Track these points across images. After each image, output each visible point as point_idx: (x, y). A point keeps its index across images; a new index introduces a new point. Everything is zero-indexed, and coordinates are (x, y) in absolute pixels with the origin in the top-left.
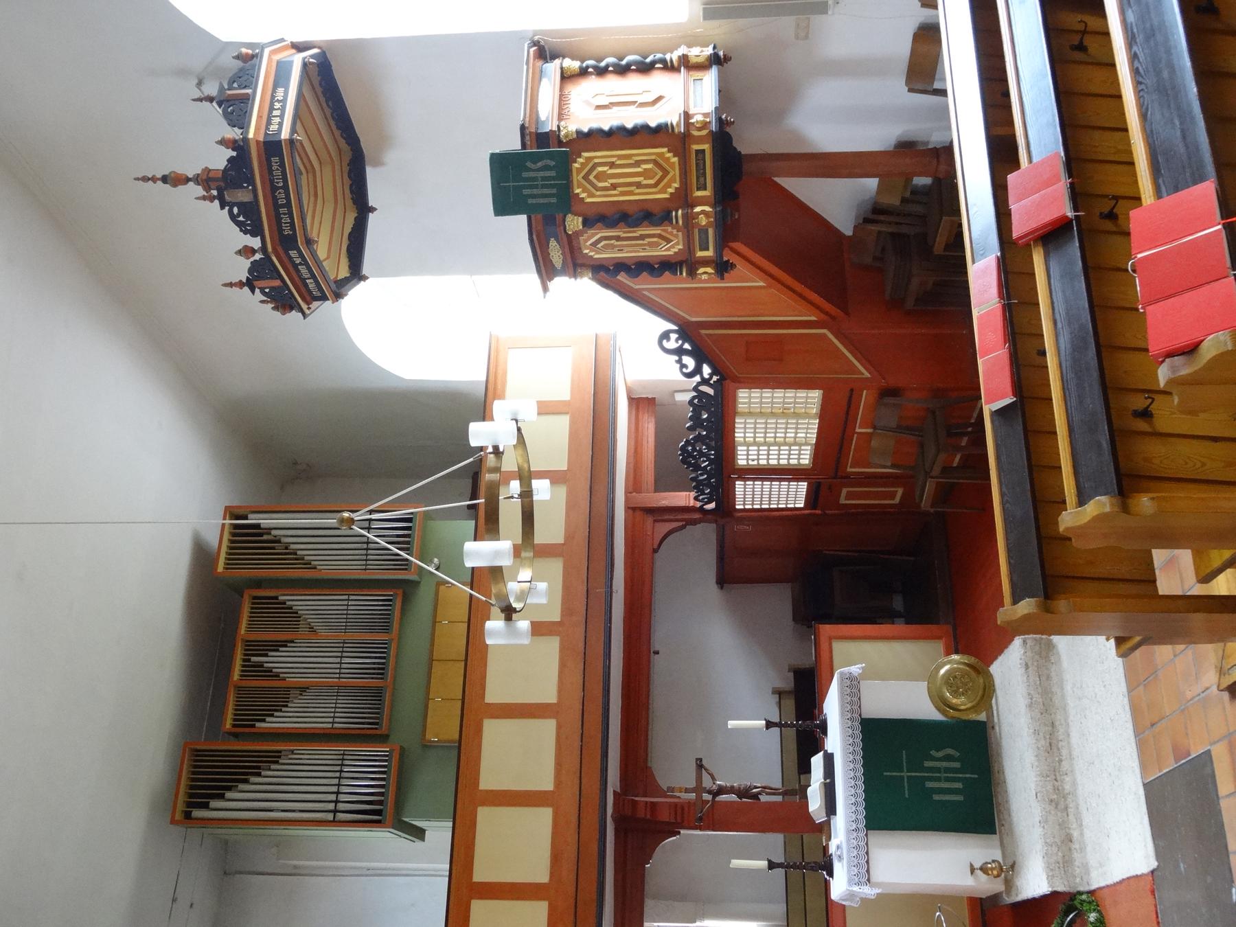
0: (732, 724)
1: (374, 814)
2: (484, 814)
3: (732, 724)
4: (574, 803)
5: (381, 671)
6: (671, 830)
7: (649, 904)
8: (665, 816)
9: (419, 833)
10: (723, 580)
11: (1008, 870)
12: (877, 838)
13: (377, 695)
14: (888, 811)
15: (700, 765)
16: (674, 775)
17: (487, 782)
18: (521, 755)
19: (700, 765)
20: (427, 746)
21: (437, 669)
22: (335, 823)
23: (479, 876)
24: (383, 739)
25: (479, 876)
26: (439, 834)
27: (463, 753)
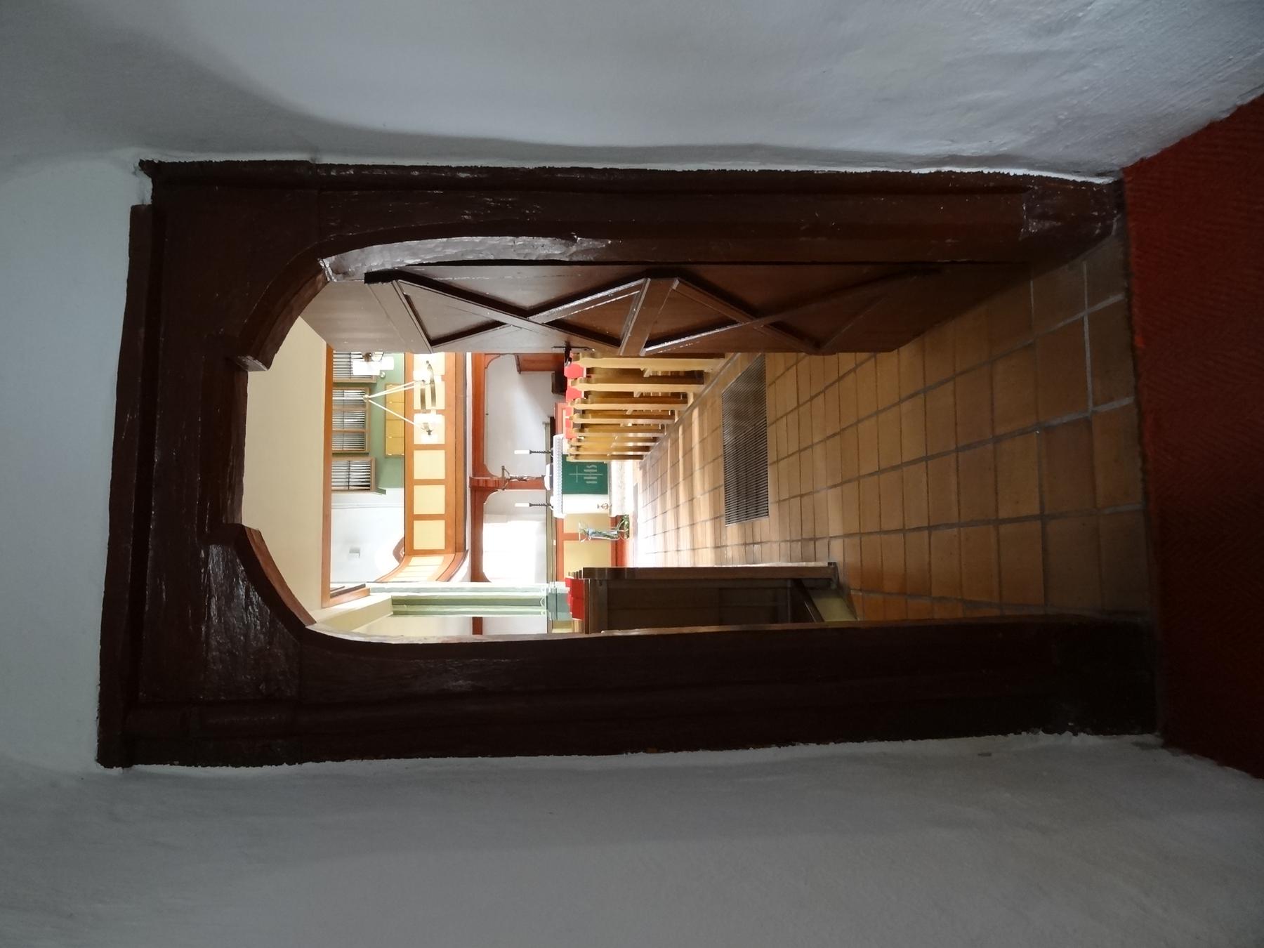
0: (516, 452)
1: (366, 487)
2: (418, 490)
3: (516, 452)
4: (452, 482)
5: (363, 423)
6: (494, 489)
7: (486, 516)
8: (491, 485)
9: (384, 492)
10: (520, 370)
11: (609, 507)
12: (565, 496)
13: (362, 435)
14: (568, 488)
15: (503, 469)
16: (495, 471)
17: (417, 476)
18: (430, 464)
19: (503, 469)
20: (387, 457)
21: (388, 423)
22: (349, 490)
23: (417, 511)
24: (367, 454)
25: (417, 511)
26: (395, 495)
27: (405, 461)
